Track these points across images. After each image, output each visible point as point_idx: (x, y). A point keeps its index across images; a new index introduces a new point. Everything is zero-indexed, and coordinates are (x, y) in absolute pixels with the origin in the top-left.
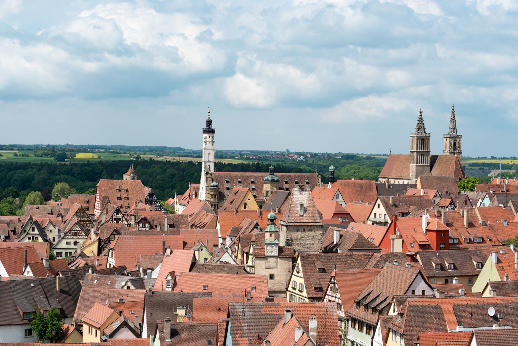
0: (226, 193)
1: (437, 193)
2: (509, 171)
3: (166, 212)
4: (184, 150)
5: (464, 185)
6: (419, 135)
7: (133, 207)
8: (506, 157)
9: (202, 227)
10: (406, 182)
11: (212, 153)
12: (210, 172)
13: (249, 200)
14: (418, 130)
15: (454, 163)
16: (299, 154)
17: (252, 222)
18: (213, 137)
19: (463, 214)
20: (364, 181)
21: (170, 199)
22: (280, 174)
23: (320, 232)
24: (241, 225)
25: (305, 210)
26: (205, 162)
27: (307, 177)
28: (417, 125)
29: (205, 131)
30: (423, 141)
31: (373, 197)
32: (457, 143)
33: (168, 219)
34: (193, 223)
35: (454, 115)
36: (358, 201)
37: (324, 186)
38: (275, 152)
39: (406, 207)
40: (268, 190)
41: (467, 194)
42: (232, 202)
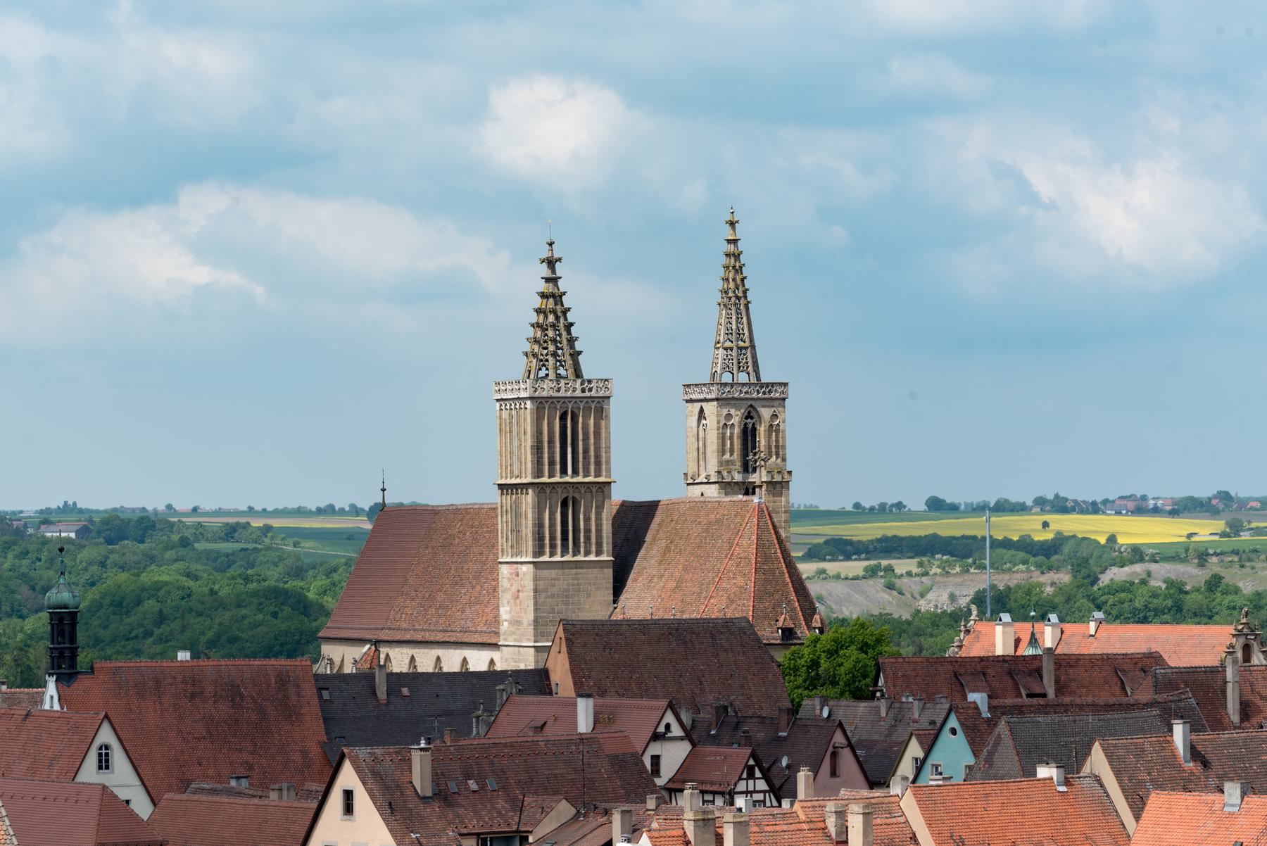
1: (669, 718)
2: (1039, 578)
5: (815, 664)
6: (547, 389)
8: (1014, 498)
10: (479, 661)
14: (543, 364)
15: (748, 544)
19: (844, 830)
28: (531, 332)
30: (569, 422)
31: (305, 753)
32: (762, 430)
35: (739, 270)
39: (501, 803)
41: (839, 716)
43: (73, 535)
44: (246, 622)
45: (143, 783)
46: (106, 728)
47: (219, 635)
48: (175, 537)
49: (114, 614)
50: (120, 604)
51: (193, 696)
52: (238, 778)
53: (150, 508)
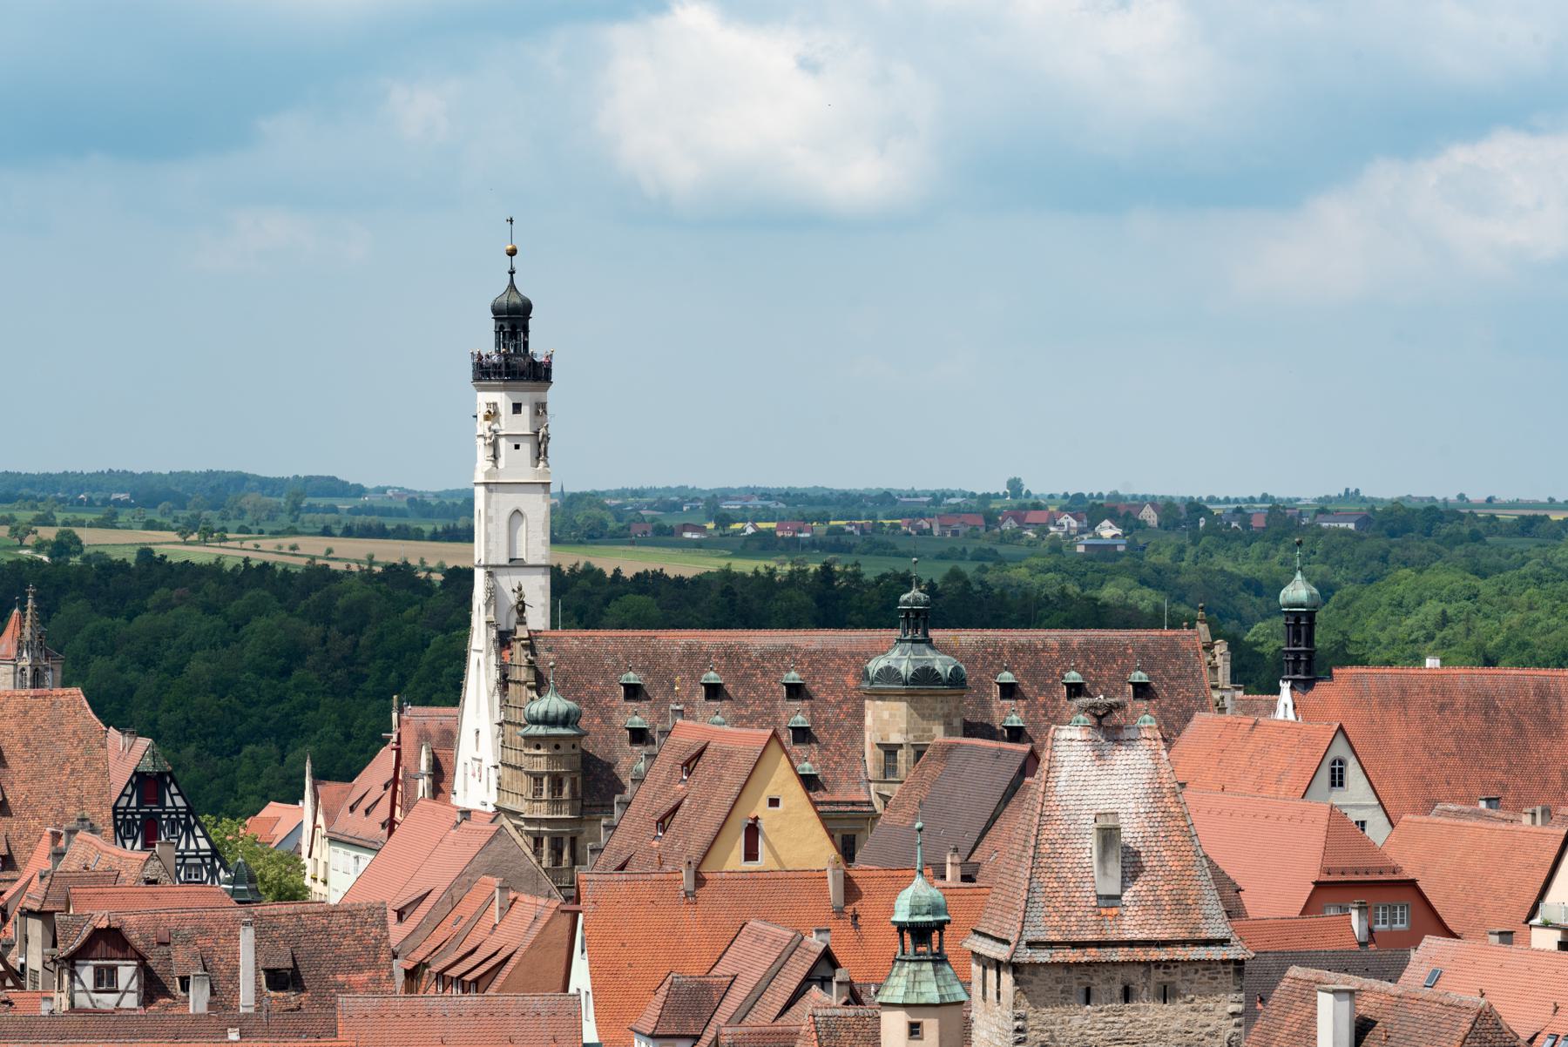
0: (630, 761)
3: (249, 887)
4: (360, 491)
7: (36, 861)
9: (478, 985)
11: (537, 509)
12: (522, 633)
13: (774, 802)
16: (1091, 510)
17: (797, 944)
18: (540, 409)
20: (1506, 674)
21: (273, 809)
22: (968, 637)
23: (1231, 1003)
24: (724, 969)
25: (1132, 867)
26: (492, 571)
27: (1143, 651)
29: (485, 373)
33: (260, 935)
34: (419, 956)
36: (1470, 800)
37: (1248, 709)
38: (937, 498)
40: (895, 738)
42: (663, 823)
43: (1352, 526)
44: (1538, 626)
45: (1381, 803)
46: (1340, 739)
47: (1508, 641)
48: (1466, 530)
49: (1393, 614)
50: (1400, 605)
51: (1442, 707)
52: (1488, 800)
53: (1439, 497)
